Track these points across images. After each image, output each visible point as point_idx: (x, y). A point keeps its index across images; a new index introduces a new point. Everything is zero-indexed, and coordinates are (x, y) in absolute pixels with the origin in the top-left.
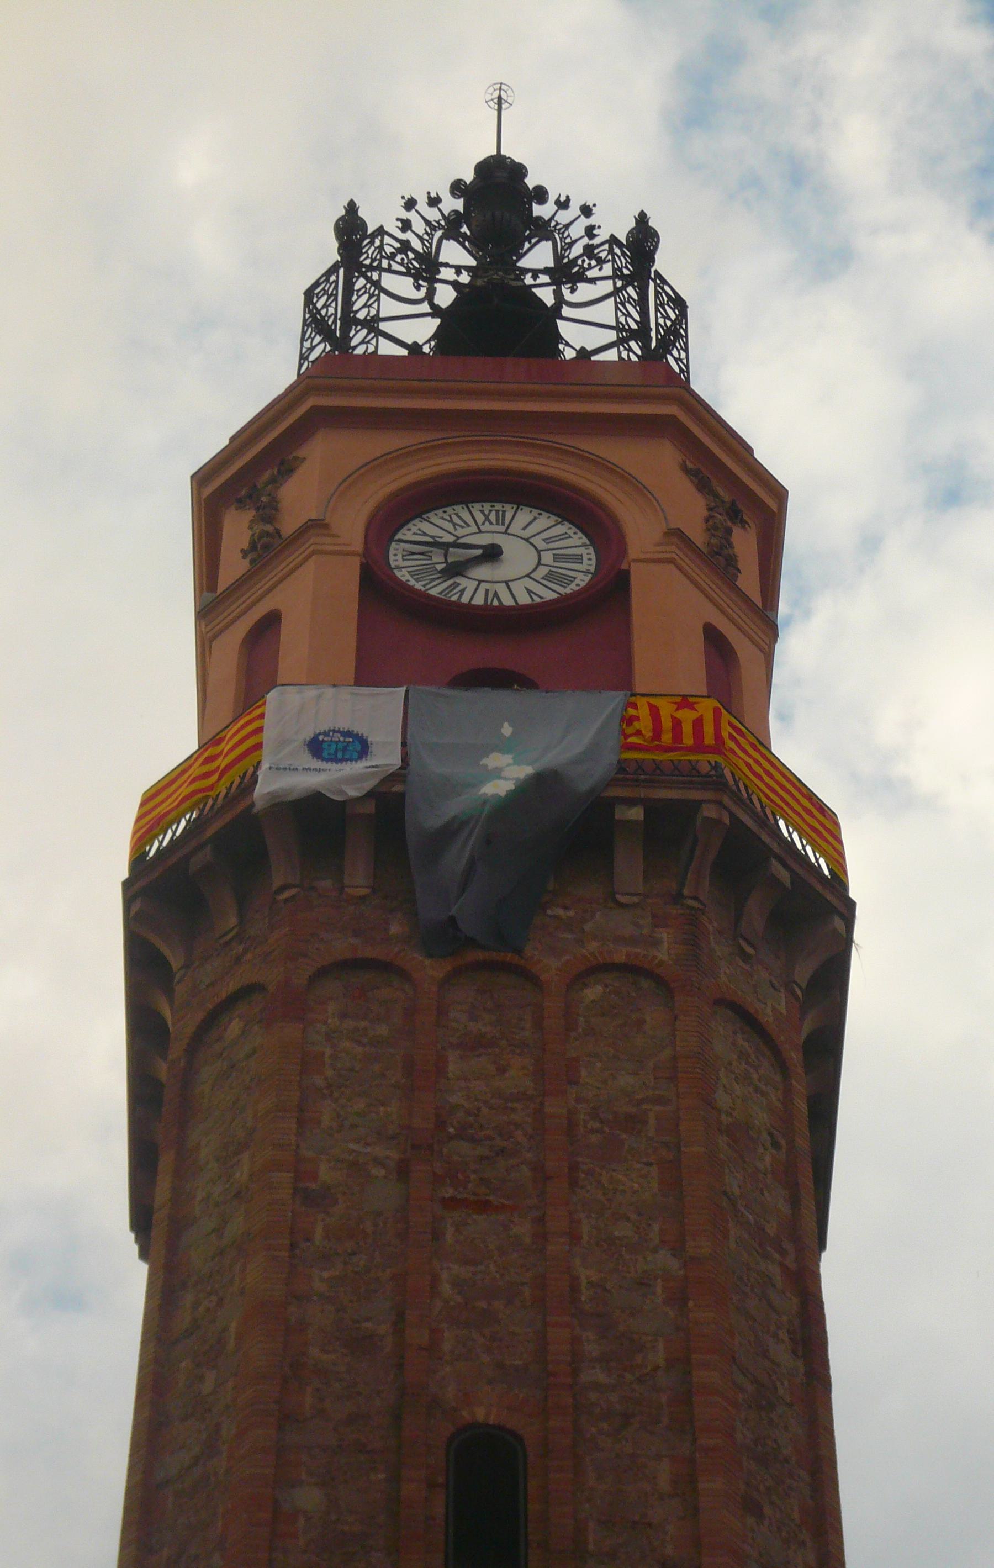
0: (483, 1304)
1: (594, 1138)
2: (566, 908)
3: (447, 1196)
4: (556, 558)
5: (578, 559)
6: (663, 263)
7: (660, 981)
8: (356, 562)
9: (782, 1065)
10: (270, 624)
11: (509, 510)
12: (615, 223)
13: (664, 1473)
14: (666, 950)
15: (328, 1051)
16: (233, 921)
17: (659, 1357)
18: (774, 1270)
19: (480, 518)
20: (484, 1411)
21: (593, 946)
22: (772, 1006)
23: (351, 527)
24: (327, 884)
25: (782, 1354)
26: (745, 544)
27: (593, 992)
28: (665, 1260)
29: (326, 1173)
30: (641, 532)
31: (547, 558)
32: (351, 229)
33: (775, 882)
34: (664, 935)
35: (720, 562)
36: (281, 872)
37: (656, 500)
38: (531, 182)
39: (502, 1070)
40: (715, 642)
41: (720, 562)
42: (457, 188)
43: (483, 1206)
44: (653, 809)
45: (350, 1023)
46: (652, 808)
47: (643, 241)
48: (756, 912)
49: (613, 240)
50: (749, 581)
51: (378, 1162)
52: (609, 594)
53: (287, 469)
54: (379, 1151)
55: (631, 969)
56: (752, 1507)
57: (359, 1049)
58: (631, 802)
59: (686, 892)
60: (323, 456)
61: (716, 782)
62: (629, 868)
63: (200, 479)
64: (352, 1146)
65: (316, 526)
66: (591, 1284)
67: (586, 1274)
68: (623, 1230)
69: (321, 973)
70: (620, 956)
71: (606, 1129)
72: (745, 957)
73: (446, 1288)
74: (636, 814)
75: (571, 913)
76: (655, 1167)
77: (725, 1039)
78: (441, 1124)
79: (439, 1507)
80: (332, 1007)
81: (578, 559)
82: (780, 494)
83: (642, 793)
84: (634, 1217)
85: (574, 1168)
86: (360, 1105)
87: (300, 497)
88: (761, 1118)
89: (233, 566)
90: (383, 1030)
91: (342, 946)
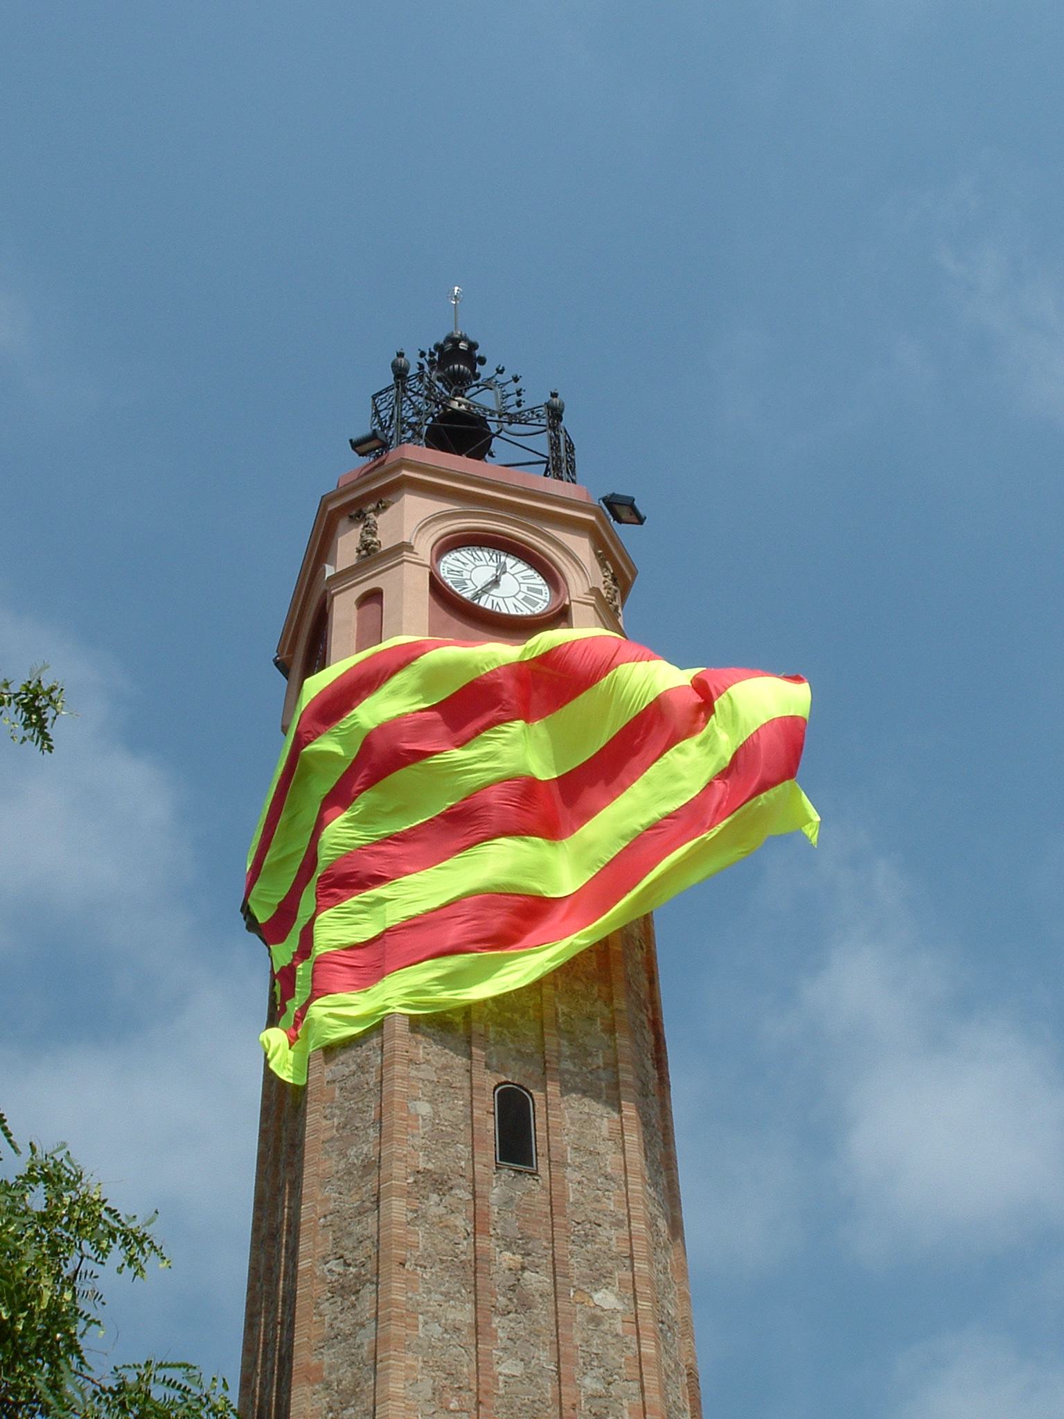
0: (508, 1015)
4: (529, 589)
8: (428, 570)
12: (535, 398)
18: (645, 1018)
19: (488, 558)
23: (424, 548)
31: (524, 588)
32: (400, 373)
47: (555, 414)
63: (325, 501)
81: (540, 592)
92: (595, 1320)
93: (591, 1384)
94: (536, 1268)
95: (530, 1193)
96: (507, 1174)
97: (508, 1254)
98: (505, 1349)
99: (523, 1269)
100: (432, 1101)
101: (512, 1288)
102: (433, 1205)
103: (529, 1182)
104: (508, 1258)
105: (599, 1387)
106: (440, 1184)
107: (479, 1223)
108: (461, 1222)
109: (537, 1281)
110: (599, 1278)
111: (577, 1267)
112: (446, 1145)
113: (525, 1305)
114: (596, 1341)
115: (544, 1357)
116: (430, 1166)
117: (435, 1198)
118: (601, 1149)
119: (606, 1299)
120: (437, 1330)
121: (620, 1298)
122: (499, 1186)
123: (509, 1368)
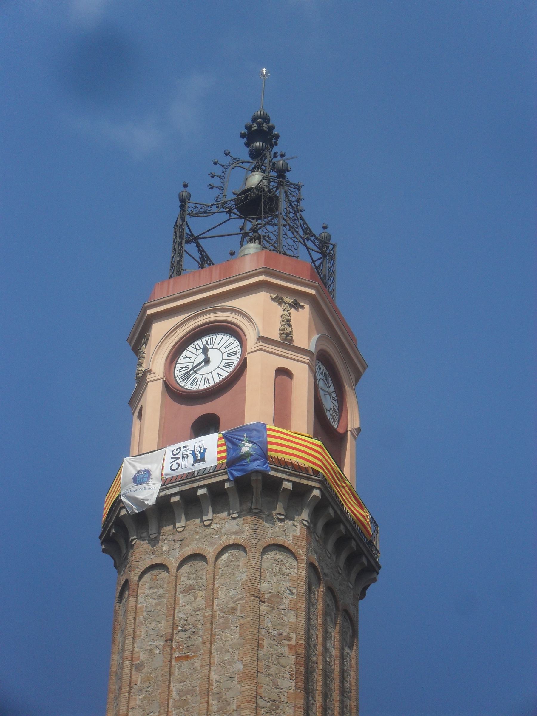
0: (184, 698)
1: (221, 620)
2: (217, 524)
3: (177, 656)
15: (145, 605)
27: (225, 557)
29: (143, 656)
31: (225, 355)
34: (246, 527)
45: (152, 591)
54: (157, 643)
57: (154, 601)
59: (253, 507)
64: (150, 643)
66: (217, 681)
68: (227, 657)
71: (225, 615)
75: (218, 526)
76: (238, 628)
80: (147, 586)
84: (230, 650)
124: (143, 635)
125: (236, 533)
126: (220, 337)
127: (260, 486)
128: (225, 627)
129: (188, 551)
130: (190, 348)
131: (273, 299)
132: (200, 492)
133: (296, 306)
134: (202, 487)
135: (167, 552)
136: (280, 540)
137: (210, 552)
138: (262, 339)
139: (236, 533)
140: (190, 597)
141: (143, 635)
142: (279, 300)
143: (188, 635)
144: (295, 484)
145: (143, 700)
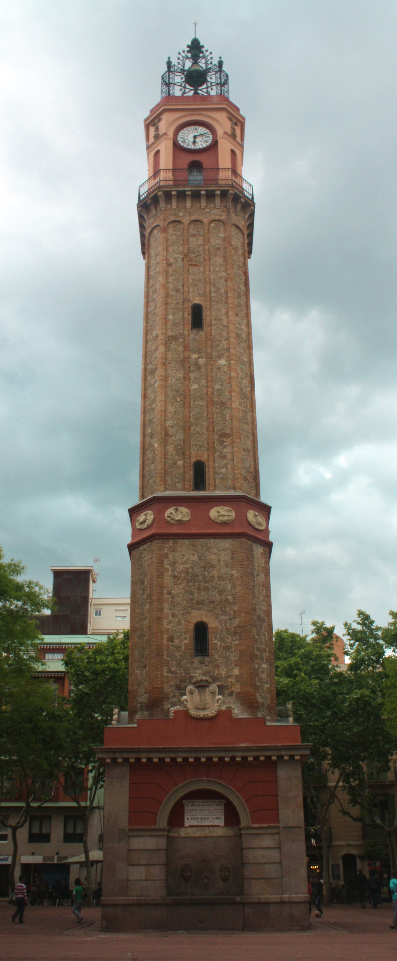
5: (209, 137)
6: (224, 68)
7: (223, 223)
9: (243, 234)
10: (158, 152)
11: (197, 127)
13: (224, 311)
14: (223, 218)
16: (154, 212)
17: (223, 291)
18: (241, 272)
20: (197, 301)
21: (212, 216)
22: (242, 224)
24: (169, 206)
25: (243, 287)
26: (238, 129)
27: (212, 225)
28: (224, 274)
29: (171, 260)
30: (220, 132)
33: (242, 202)
34: (224, 214)
35: (233, 136)
36: (162, 205)
37: (222, 123)
38: (201, 44)
39: (198, 240)
40: (233, 152)
41: (233, 136)
42: (188, 46)
43: (196, 265)
44: (222, 191)
45: (174, 232)
46: (222, 191)
48: (239, 207)
49: (215, 65)
50: (238, 139)
51: (179, 258)
52: (214, 145)
53: (160, 120)
55: (219, 220)
56: (237, 315)
58: (218, 190)
60: (166, 118)
61: (232, 186)
62: (218, 201)
63: (146, 120)
65: (165, 134)
67: (212, 277)
68: (217, 269)
69: (169, 223)
70: (217, 218)
72: (237, 215)
73: (190, 280)
74: (219, 192)
77: (234, 231)
78: (189, 250)
79: (190, 318)
82: (244, 119)
83: (220, 188)
85: (210, 258)
86: (176, 247)
87: (162, 126)
88: (239, 245)
89: (152, 140)
90: (179, 233)
91: (172, 218)
92: (219, 368)
93: (217, 387)
94: (202, 357)
95: (201, 336)
96: (194, 331)
97: (194, 355)
98: (193, 382)
99: (199, 358)
100: (173, 314)
101: (195, 364)
102: (173, 345)
103: (201, 333)
104: (195, 356)
105: (219, 387)
106: (175, 338)
107: (186, 347)
108: (181, 348)
109: (202, 361)
110: (220, 357)
111: (215, 354)
112: (177, 327)
113: (199, 368)
114: (219, 374)
115: (203, 382)
116: (173, 334)
117: (174, 343)
118: (222, 318)
119: (222, 362)
120: (174, 380)
121: (226, 361)
122: (194, 336)
123: (195, 386)
124: (171, 251)
125: (218, 215)
126: (200, 128)
127: (232, 197)
128: (215, 255)
129: (194, 218)
130: (185, 129)
131: (228, 118)
132: (202, 192)
133: (236, 124)
134: (203, 190)
135: (182, 217)
136: (238, 224)
137: (206, 221)
138: (226, 133)
139: (218, 215)
140: (195, 239)
141: (171, 251)
142: (230, 120)
143: (195, 255)
144: (245, 201)
145: (174, 279)
